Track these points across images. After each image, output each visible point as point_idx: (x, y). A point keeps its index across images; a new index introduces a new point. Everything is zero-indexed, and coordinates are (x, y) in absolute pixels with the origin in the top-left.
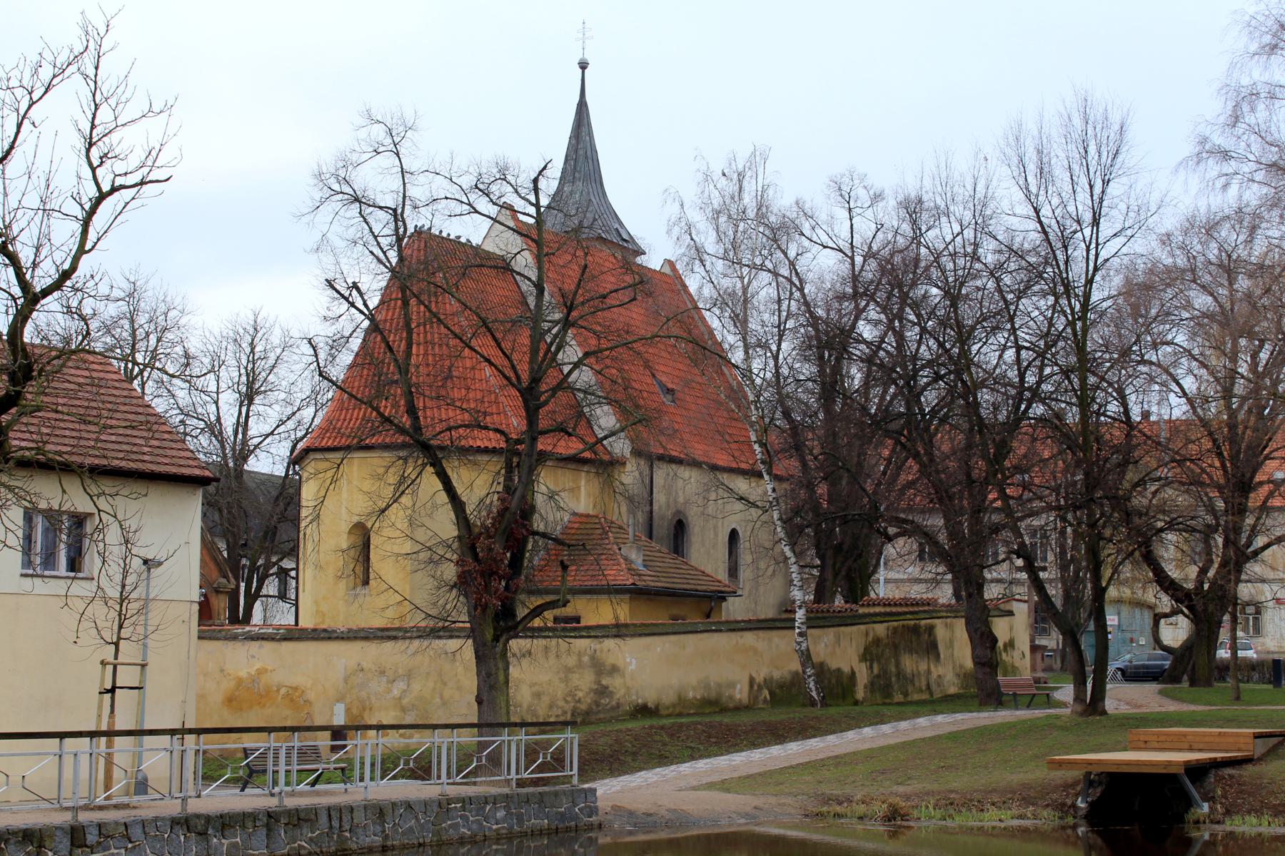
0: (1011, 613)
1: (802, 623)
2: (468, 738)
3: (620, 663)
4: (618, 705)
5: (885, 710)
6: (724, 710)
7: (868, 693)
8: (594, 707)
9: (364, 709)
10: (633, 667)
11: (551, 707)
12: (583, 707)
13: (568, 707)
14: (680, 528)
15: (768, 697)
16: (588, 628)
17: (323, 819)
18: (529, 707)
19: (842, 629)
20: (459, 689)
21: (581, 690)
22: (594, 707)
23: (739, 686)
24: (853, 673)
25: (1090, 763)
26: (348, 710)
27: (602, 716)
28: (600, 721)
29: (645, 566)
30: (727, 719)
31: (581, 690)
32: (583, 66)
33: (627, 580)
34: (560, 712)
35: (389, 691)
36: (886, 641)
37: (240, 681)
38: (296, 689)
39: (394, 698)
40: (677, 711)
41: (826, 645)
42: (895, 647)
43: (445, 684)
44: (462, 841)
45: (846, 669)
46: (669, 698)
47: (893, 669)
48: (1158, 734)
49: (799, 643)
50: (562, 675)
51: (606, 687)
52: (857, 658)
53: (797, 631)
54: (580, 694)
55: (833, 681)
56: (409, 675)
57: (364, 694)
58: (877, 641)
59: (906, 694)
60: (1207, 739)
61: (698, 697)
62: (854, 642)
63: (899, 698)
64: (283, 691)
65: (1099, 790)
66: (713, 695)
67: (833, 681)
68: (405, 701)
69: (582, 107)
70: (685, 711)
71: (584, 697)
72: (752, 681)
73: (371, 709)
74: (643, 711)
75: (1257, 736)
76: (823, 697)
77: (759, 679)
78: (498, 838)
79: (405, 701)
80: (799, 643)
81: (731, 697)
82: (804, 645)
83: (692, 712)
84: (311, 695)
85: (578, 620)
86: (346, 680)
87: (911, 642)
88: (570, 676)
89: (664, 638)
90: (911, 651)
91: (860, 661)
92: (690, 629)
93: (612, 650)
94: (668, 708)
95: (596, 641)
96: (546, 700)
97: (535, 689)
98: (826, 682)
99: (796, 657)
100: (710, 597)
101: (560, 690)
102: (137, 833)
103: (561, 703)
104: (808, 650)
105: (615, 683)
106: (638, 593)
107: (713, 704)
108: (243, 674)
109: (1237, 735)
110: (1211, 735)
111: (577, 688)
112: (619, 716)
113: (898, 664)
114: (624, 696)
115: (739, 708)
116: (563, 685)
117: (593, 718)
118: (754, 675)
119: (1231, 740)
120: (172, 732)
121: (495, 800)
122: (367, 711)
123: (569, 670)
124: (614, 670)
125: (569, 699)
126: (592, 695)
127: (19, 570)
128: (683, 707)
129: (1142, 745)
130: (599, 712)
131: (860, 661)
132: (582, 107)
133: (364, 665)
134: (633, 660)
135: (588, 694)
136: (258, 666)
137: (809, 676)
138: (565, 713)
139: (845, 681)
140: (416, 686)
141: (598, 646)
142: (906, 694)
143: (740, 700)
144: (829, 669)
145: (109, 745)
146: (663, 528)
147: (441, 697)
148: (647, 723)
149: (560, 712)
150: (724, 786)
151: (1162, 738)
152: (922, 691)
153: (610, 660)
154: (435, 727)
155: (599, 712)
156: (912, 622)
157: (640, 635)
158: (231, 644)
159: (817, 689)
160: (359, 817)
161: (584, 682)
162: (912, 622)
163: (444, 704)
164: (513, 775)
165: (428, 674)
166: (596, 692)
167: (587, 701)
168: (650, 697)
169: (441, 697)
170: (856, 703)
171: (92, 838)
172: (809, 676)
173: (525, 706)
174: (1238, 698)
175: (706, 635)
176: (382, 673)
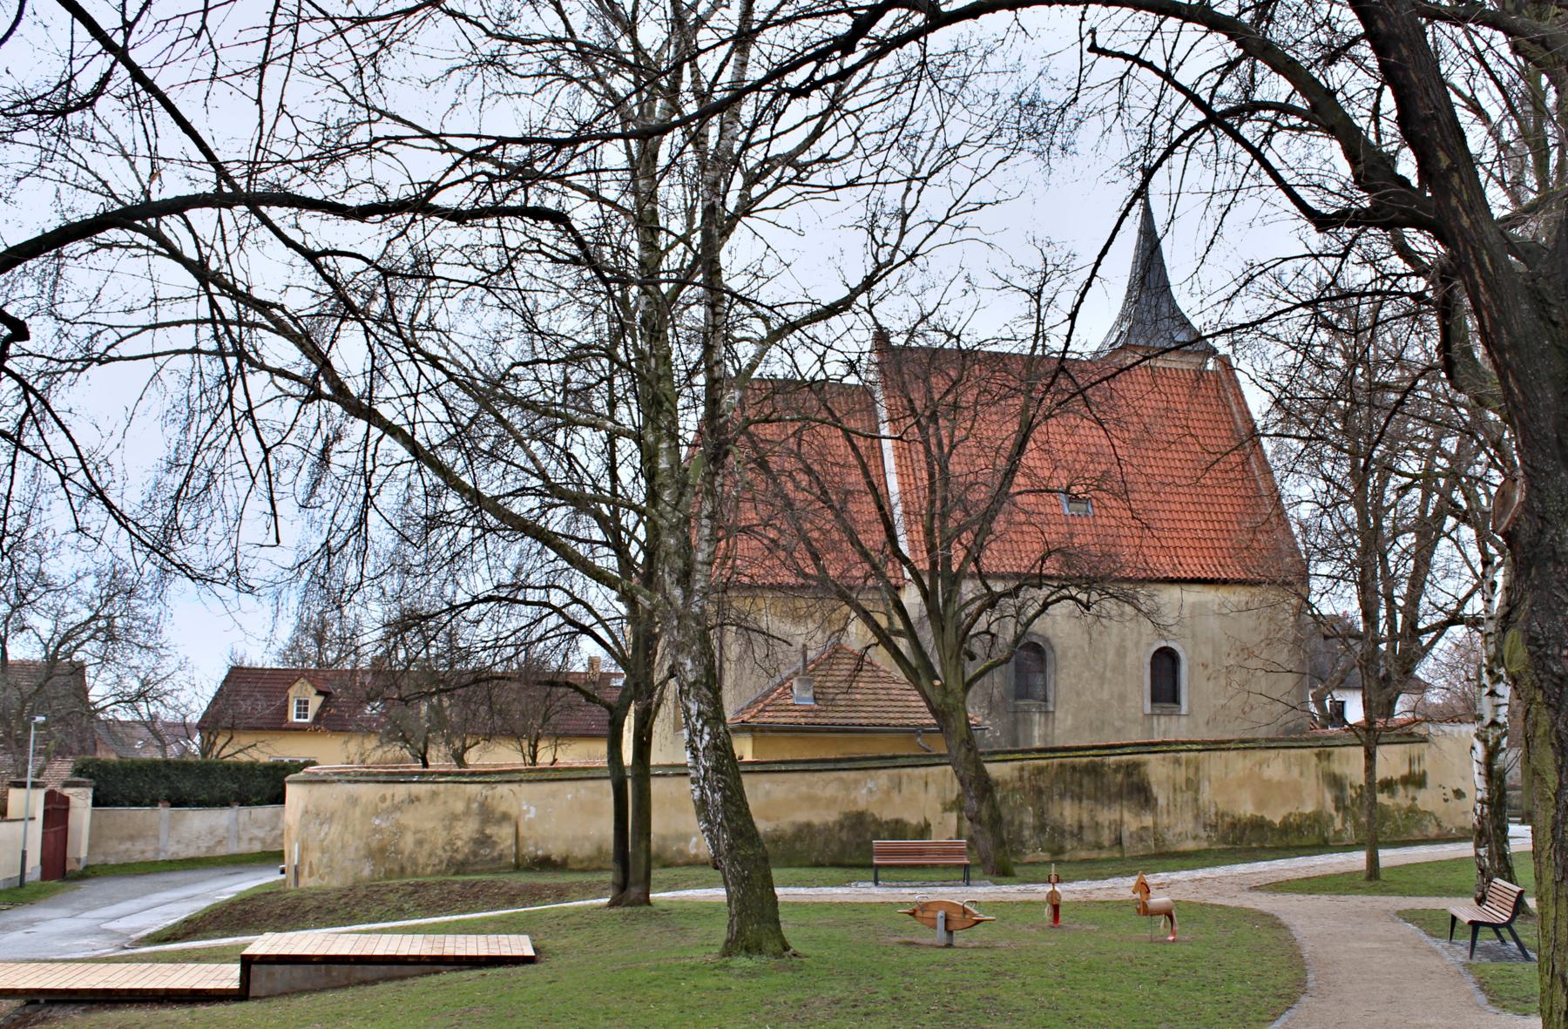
3: (514, 811)
4: (501, 857)
11: (430, 855)
12: (459, 857)
13: (445, 856)
18: (410, 857)
28: (476, 872)
36: (1018, 784)
40: (595, 865)
41: (870, 791)
47: (1029, 819)
51: (490, 837)
52: (939, 807)
54: (459, 843)
62: (932, 789)
81: (681, 852)
87: (1081, 785)
89: (579, 784)
91: (947, 808)
93: (506, 796)
94: (582, 861)
97: (419, 836)
101: (441, 837)
103: (440, 852)
105: (504, 834)
111: (458, 837)
113: (1041, 814)
117: (470, 868)
123: (455, 817)
124: (505, 817)
131: (947, 808)
134: (533, 809)
143: (696, 856)
144: (875, 821)
152: (1100, 847)
153: (503, 807)
156: (1085, 760)
161: (467, 830)
162: (1085, 760)
167: (464, 848)
168: (556, 850)
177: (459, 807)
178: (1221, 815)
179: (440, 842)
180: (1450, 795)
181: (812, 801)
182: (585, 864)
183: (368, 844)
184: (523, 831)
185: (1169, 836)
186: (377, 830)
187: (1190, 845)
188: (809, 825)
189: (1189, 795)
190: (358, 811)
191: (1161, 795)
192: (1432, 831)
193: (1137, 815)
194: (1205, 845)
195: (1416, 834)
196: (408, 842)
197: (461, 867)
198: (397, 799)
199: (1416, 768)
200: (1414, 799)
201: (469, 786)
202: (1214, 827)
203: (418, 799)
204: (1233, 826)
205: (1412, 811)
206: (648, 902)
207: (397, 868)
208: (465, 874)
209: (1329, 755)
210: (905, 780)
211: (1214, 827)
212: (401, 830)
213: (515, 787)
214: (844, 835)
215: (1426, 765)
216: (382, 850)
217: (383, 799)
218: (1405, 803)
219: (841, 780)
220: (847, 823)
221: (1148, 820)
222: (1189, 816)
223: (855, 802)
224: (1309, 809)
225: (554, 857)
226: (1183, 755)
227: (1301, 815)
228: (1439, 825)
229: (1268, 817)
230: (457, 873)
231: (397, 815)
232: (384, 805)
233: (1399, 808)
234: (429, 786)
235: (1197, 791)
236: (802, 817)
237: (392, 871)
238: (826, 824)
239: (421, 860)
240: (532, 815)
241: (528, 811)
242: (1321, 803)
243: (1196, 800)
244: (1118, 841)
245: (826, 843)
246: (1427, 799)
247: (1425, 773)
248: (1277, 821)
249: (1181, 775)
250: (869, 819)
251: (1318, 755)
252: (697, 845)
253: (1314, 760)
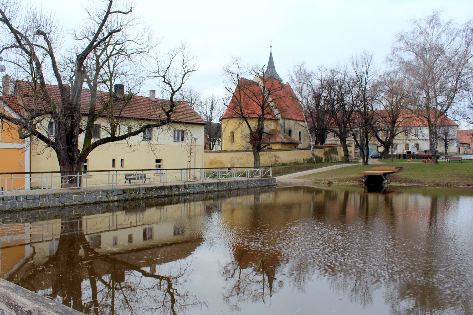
0: (351, 146)
2: (252, 169)
3: (280, 156)
5: (328, 164)
6: (298, 164)
13: (270, 164)
14: (290, 131)
17: (227, 184)
25: (365, 173)
26: (231, 165)
28: (276, 166)
30: (299, 166)
32: (271, 47)
33: (280, 141)
37: (212, 160)
42: (330, 152)
44: (252, 188)
45: (321, 157)
46: (288, 162)
56: (242, 158)
58: (326, 152)
59: (332, 161)
63: (330, 162)
65: (367, 178)
66: (296, 162)
68: (241, 163)
69: (271, 54)
72: (303, 159)
74: (284, 164)
77: (305, 159)
78: (258, 187)
84: (224, 162)
85: (272, 148)
86: (230, 159)
90: (333, 153)
93: (278, 153)
96: (266, 162)
101: (269, 161)
102: (195, 186)
105: (279, 159)
106: (283, 143)
107: (296, 163)
108: (212, 158)
113: (330, 156)
115: (301, 164)
120: (200, 169)
121: (258, 180)
123: (270, 157)
124: (278, 157)
127: (173, 141)
128: (291, 164)
132: (271, 54)
140: (243, 160)
142: (332, 161)
145: (190, 171)
146: (287, 131)
148: (284, 167)
150: (299, 178)
153: (278, 155)
154: (246, 167)
158: (210, 153)
160: (233, 183)
161: (273, 159)
163: (248, 163)
164: (261, 176)
168: (285, 162)
170: (323, 163)
171: (187, 187)
174: (393, 161)
176: (237, 158)
244: (336, 160)
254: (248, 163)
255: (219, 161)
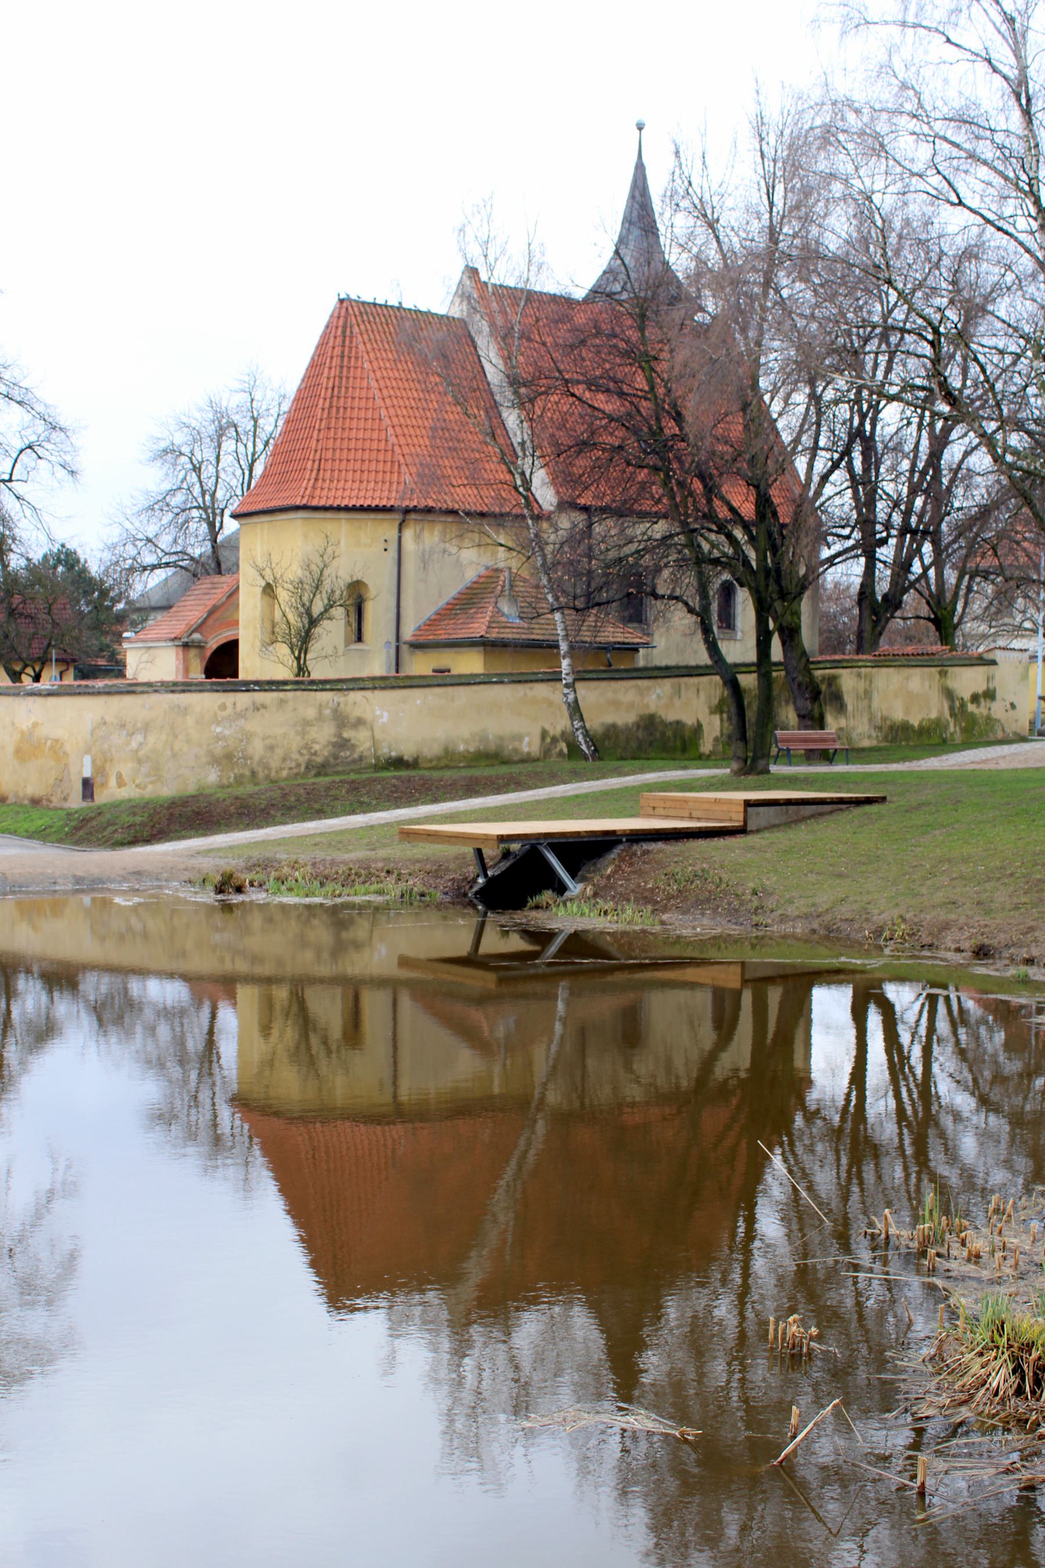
0: (993, 663)
1: (567, 674)
3: (368, 716)
4: (361, 758)
7: (720, 748)
8: (332, 760)
9: (106, 761)
10: (385, 719)
11: (284, 760)
12: (319, 760)
13: (302, 761)
15: (565, 750)
16: (313, 682)
18: (261, 761)
19: (686, 679)
20: (188, 741)
21: (318, 743)
22: (332, 760)
23: (527, 739)
24: (700, 725)
26: (93, 762)
27: (340, 769)
28: (338, 773)
29: (521, 618)
31: (318, 743)
32: (640, 127)
34: (293, 765)
35: (128, 744)
37: (23, 733)
38: (57, 741)
39: (132, 751)
40: (443, 763)
41: (659, 697)
43: (176, 737)
45: (689, 720)
48: (665, 800)
49: (565, 695)
50: (299, 729)
52: (707, 711)
53: (564, 682)
54: (317, 747)
55: (669, 733)
56: (146, 728)
57: (106, 746)
60: (706, 806)
61: (472, 750)
62: (702, 695)
64: (49, 743)
66: (492, 747)
67: (669, 733)
68: (141, 753)
69: (640, 168)
70: (453, 764)
71: (321, 750)
72: (544, 734)
73: (111, 761)
74: (399, 763)
75: (748, 804)
76: (596, 750)
79: (141, 753)
80: (565, 695)
81: (516, 751)
82: (571, 697)
83: (462, 765)
84: (68, 748)
85: (449, 671)
88: (308, 729)
89: (427, 690)
91: (712, 712)
92: (463, 681)
94: (431, 761)
95: (340, 694)
96: (279, 752)
97: (268, 742)
98: (658, 735)
99: (565, 708)
100: (605, 648)
101: (295, 742)
103: (295, 756)
104: (576, 701)
105: (361, 739)
106: (488, 645)
108: (24, 727)
109: (730, 802)
110: (708, 801)
111: (314, 741)
112: (361, 769)
114: (369, 749)
116: (299, 738)
117: (330, 770)
118: (547, 727)
119: (725, 808)
122: (108, 763)
123: (307, 723)
124: (360, 722)
125: (304, 751)
126: (330, 747)
128: (449, 759)
129: (651, 812)
130: (338, 764)
131: (712, 712)
132: (640, 168)
133: (108, 719)
134: (386, 714)
135: (325, 747)
136: (33, 719)
137: (577, 730)
138: (298, 765)
139: (687, 734)
140: (151, 739)
141: (342, 699)
143: (529, 753)
144: (662, 722)
147: (172, 749)
148: (404, 773)
149: (293, 765)
151: (668, 804)
153: (356, 713)
155: (338, 764)
157: (393, 688)
159: (586, 742)
161: (323, 736)
163: (174, 755)
165: (162, 727)
166: (334, 745)
168: (408, 751)
169: (172, 749)
172: (577, 730)
173: (256, 758)
175: (482, 687)
176: (123, 726)
177: (311, 713)
178: (884, 719)
179: (295, 747)
180: (1009, 707)
181: (616, 704)
182: (434, 763)
183: (210, 753)
184: (378, 735)
185: (854, 735)
186: (219, 738)
187: (866, 743)
188: (614, 726)
189: (865, 703)
190: (190, 721)
191: (849, 700)
192: (1000, 735)
193: (836, 718)
194: (874, 743)
195: (992, 737)
196: (257, 749)
197: (322, 769)
198: (239, 708)
199: (991, 686)
200: (990, 709)
201: (319, 694)
202: (880, 728)
203: (264, 707)
204: (891, 727)
205: (989, 718)
206: (768, 772)
207: (248, 773)
208: (326, 775)
209: (946, 673)
210: (683, 686)
211: (880, 728)
212: (248, 737)
213: (368, 694)
214: (640, 734)
215: (995, 684)
216: (229, 757)
217: (223, 707)
218: (985, 712)
219: (637, 687)
220: (641, 724)
221: (843, 723)
222: (865, 720)
223: (647, 706)
224: (934, 715)
225: (406, 758)
226: (863, 670)
227: (929, 720)
228: (1003, 730)
229: (911, 722)
230: (318, 775)
231: (242, 722)
232: (225, 713)
233: (981, 713)
234: (275, 694)
235: (870, 700)
236: (609, 718)
237: (242, 776)
238: (627, 725)
239: (274, 764)
240: (385, 719)
241: (381, 716)
242: (941, 712)
243: (870, 707)
245: (628, 741)
246: (997, 710)
247: (995, 689)
248: (916, 724)
249: (862, 685)
250: (658, 720)
251: (940, 673)
252: (530, 744)
253: (937, 676)
254: (174, 755)
255: (47, 739)
